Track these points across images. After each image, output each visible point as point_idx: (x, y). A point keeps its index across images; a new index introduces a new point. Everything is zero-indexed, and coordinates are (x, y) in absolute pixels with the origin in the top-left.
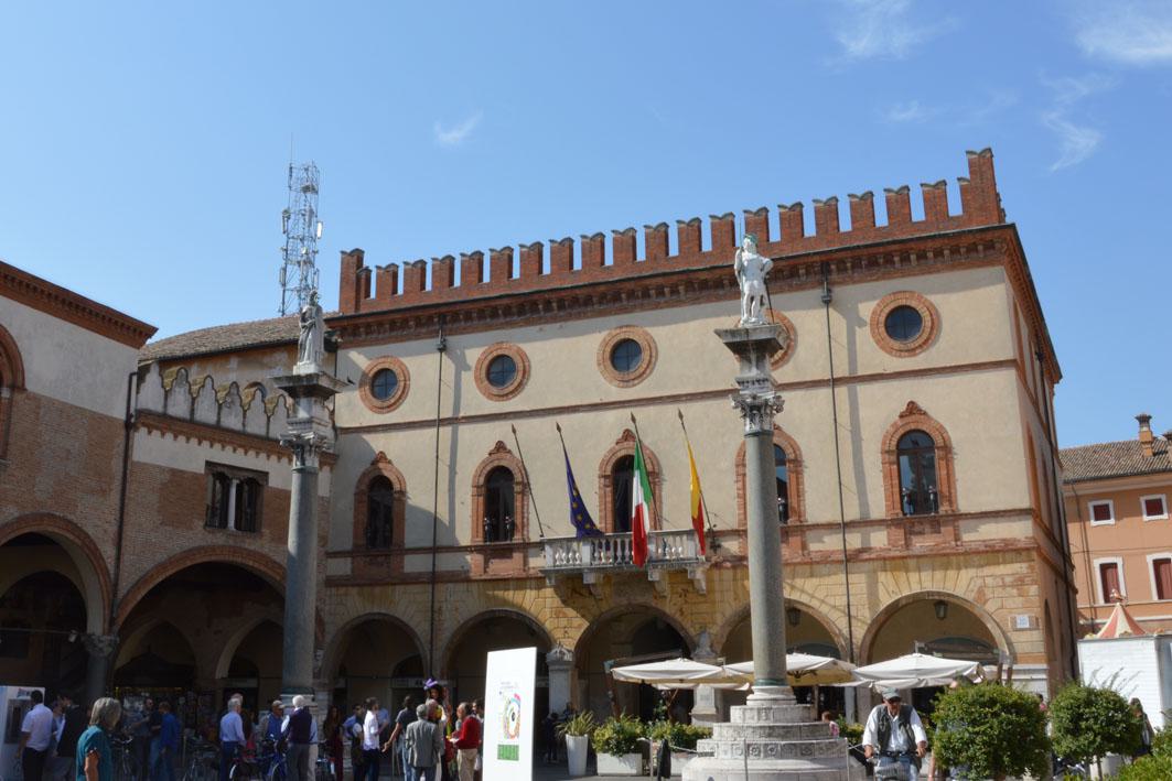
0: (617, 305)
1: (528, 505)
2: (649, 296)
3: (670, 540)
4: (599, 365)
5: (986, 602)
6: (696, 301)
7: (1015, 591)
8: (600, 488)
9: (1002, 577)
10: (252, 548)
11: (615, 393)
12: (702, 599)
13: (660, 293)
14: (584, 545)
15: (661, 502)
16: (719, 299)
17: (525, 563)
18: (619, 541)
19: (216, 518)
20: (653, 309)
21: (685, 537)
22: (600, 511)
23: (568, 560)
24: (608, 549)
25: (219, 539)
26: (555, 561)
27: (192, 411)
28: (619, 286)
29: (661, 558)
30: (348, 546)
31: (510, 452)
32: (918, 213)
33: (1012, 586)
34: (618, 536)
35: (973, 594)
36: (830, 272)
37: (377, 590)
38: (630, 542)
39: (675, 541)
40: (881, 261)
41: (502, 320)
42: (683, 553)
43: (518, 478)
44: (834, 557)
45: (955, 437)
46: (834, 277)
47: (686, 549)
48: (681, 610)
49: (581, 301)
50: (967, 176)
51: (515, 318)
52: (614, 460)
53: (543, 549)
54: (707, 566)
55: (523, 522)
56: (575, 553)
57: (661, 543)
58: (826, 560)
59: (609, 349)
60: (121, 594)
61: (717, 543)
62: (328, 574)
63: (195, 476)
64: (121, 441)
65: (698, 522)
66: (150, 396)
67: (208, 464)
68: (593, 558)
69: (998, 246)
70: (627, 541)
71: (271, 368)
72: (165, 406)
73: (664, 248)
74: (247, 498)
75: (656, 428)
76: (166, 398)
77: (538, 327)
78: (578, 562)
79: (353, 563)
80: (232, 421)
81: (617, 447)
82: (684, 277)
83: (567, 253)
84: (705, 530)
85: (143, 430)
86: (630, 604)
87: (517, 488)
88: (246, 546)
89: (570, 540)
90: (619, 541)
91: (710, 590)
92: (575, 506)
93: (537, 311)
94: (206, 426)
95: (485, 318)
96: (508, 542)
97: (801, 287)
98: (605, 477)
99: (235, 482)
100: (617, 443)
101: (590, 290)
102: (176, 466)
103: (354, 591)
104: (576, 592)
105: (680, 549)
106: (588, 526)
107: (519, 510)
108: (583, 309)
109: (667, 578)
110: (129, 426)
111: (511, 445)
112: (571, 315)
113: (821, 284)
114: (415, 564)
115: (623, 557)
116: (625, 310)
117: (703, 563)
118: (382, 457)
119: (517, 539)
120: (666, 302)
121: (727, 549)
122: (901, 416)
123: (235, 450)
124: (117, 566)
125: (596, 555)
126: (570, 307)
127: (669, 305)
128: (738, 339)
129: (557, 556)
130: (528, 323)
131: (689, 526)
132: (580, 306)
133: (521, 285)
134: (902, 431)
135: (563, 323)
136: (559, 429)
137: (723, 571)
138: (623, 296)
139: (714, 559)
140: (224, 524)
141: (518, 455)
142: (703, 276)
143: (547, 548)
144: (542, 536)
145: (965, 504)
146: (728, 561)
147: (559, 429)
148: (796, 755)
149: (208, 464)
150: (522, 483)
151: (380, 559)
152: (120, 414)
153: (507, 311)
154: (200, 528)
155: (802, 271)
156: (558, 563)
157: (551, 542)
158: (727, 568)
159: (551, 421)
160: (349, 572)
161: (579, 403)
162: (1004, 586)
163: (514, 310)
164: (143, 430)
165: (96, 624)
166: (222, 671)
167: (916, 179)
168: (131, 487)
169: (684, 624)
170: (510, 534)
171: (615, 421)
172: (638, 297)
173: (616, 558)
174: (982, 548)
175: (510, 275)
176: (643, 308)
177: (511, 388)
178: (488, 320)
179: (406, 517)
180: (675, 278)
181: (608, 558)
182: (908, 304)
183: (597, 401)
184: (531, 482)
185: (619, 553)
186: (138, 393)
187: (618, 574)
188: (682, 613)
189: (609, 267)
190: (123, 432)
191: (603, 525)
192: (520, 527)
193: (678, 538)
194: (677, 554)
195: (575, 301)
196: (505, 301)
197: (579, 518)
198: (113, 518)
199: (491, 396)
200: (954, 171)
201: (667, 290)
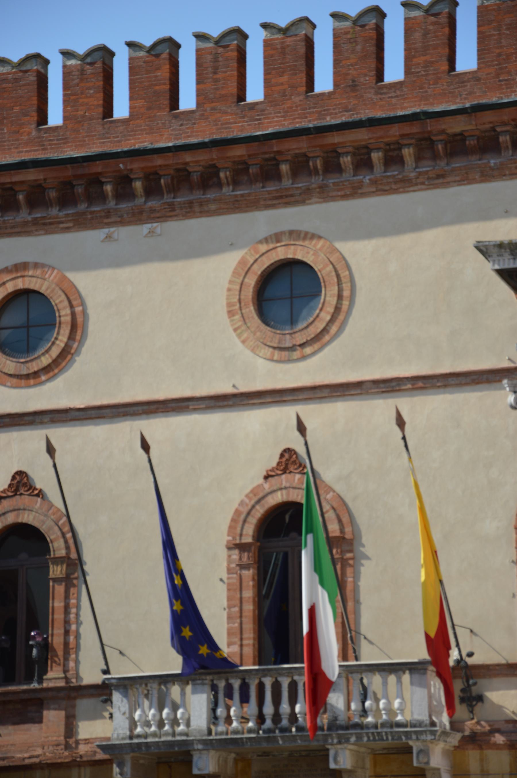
0: (272, 187)
1: (78, 607)
2: (339, 169)
3: (375, 682)
4: (231, 313)
6: (439, 180)
8: (229, 571)
13: (363, 163)
14: (194, 692)
15: (357, 602)
16: (487, 176)
17: (70, 730)
18: (268, 682)
20: (345, 197)
21: (406, 677)
22: (230, 618)
23: (161, 724)
24: (245, 699)
26: (133, 724)
28: (276, 146)
29: (356, 720)
31: (40, 494)
34: (265, 673)
38: (293, 686)
39: (385, 683)
41: (24, 215)
42: (402, 710)
43: (58, 548)
47: (411, 702)
49: (195, 177)
51: (54, 211)
52: (260, 511)
53: (108, 700)
54: (455, 739)
55: (66, 644)
56: (175, 708)
57: (356, 690)
59: (252, 281)
61: (475, 691)
65: (439, 642)
68: (214, 718)
70: (285, 682)
73: (446, 51)
75: (352, 452)
77: (101, 234)
78: (182, 728)
81: (267, 486)
82: (415, 129)
83: (164, 73)
84: (451, 662)
87: (56, 571)
90: (268, 682)
92: (178, 607)
93: (103, 197)
96: (35, 685)
98: (242, 547)
101: (215, 154)
105: (396, 703)
106: (204, 650)
107: (59, 616)
108: (197, 195)
109: (368, 764)
111: (42, 478)
112: (172, 207)
115: (277, 717)
116: (284, 199)
117: (444, 733)
119: (54, 678)
120: (374, 182)
121: (500, 707)
125: (220, 711)
126: (174, 189)
127: (382, 188)
129: (137, 715)
130: (81, 223)
131: (420, 653)
132: (191, 189)
133: (65, 141)
136: (145, 446)
137: (490, 753)
138: (284, 168)
139: (469, 725)
141: (59, 504)
142: (457, 126)
143: (116, 697)
144: (106, 672)
146: (498, 731)
147: (145, 446)
150: (66, 560)
153: (37, 197)
156: (139, 730)
157: (127, 684)
158: (496, 746)
159: (128, 430)
161: (187, 393)
163: (53, 194)
170: (39, 666)
171: (264, 431)
172: (316, 172)
173: (261, 719)
175: (42, 117)
176: (325, 194)
177: (45, 361)
180: (395, 131)
181: (244, 719)
183: (226, 389)
184: (87, 557)
185: (268, 709)
187: (265, 754)
189: (254, 105)
191: (236, 648)
192: (60, 653)
193: (392, 679)
194: (390, 711)
195: (182, 179)
196: (31, 175)
197: (187, 633)
201: (376, 156)
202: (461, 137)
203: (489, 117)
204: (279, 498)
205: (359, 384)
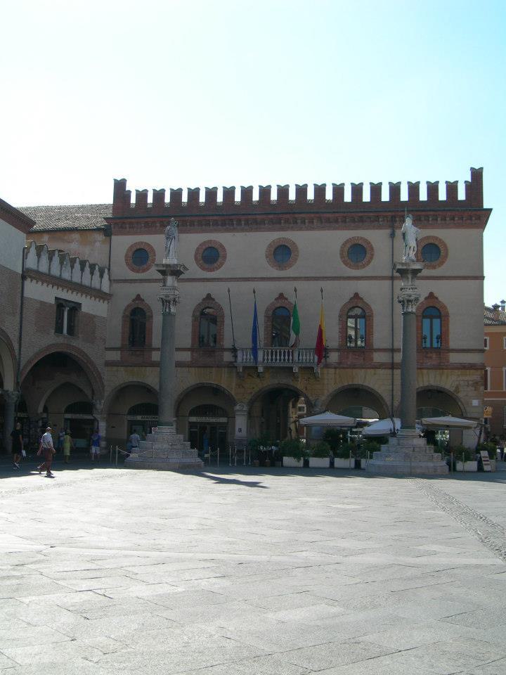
6: (323, 228)
7: (474, 388)
11: (276, 273)
13: (303, 222)
16: (335, 229)
19: (59, 329)
25: (60, 340)
26: (243, 360)
30: (118, 344)
36: (396, 221)
37: (136, 369)
45: (451, 310)
48: (306, 388)
51: (220, 227)
58: (381, 366)
59: (273, 249)
60: (21, 368)
63: (51, 305)
64: (20, 285)
66: (31, 262)
67: (57, 299)
71: (69, 242)
72: (38, 266)
74: (66, 315)
77: (232, 234)
79: (121, 354)
80: (66, 275)
82: (317, 215)
85: (29, 279)
88: (72, 344)
94: (54, 277)
95: (202, 225)
97: (380, 227)
100: (276, 299)
101: (264, 216)
102: (42, 300)
103: (122, 369)
104: (251, 376)
110: (24, 278)
118: (138, 297)
122: (426, 298)
123: (67, 291)
124: (20, 354)
130: (227, 230)
135: (247, 233)
140: (61, 332)
148: (240, 462)
149: (57, 299)
151: (138, 353)
152: (20, 271)
153: (216, 223)
162: (468, 386)
163: (220, 223)
164: (29, 279)
165: (9, 385)
166: (40, 409)
167: (442, 178)
168: (25, 311)
176: (292, 229)
178: (204, 227)
186: (26, 258)
196: (215, 218)
198: (17, 328)
199: (203, 269)
201: (306, 221)
202: (329, 218)
203: (337, 215)
204: (279, 305)
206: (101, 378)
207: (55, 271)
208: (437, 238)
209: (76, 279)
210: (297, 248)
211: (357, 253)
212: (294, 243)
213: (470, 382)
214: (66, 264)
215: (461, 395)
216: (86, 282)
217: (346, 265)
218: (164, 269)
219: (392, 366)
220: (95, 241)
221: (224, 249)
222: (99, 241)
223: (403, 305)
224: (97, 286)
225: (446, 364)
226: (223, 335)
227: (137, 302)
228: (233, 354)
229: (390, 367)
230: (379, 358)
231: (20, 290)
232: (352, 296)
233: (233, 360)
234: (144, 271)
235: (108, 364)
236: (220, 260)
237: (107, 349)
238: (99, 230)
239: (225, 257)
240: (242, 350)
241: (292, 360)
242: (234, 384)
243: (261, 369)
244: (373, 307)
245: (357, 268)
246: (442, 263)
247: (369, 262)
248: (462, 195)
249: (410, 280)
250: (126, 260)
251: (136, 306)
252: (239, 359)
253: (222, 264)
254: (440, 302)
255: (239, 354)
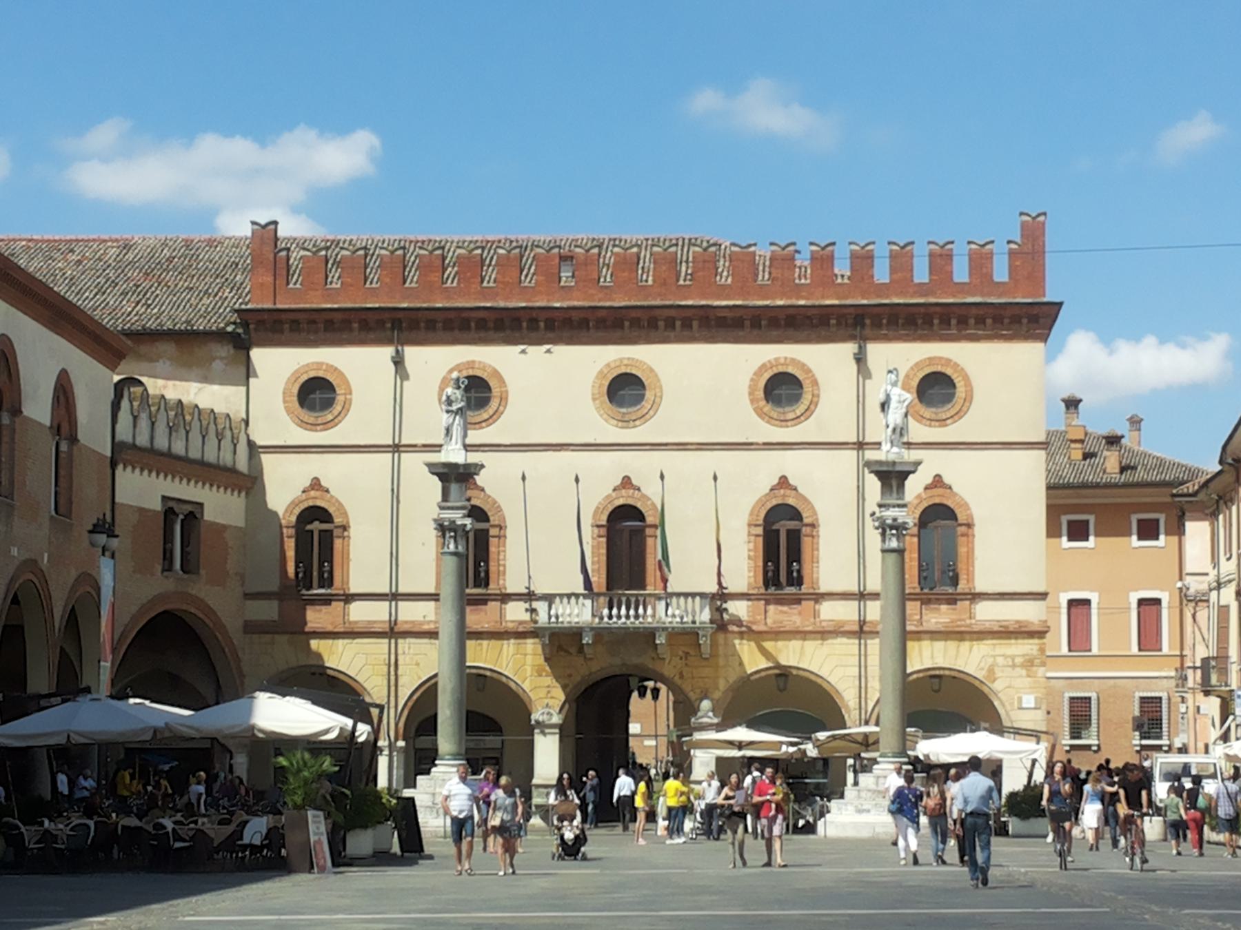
4: (594, 399)
5: (994, 681)
7: (1024, 672)
8: (593, 538)
9: (1013, 657)
10: (194, 592)
12: (704, 663)
26: (550, 617)
27: (152, 438)
32: (961, 272)
33: (1022, 666)
35: (984, 672)
36: (863, 326)
40: (920, 321)
44: (847, 628)
46: (867, 331)
50: (1018, 240)
51: (491, 333)
52: (610, 508)
62: (247, 618)
67: (164, 498)
69: (1042, 321)
76: (135, 426)
79: (280, 607)
80: (179, 448)
81: (614, 495)
86: (624, 664)
89: (577, 596)
91: (714, 655)
99: (181, 517)
103: (284, 638)
113: (851, 338)
114: (360, 612)
122: (926, 488)
128: (885, 469)
134: (925, 504)
138: (627, 324)
145: (981, 584)
149: (164, 498)
152: (109, 454)
154: (159, 573)
155: (833, 322)
160: (276, 618)
162: (1014, 666)
164: (120, 467)
169: (684, 686)
174: (996, 628)
177: (485, 416)
179: (351, 556)
182: (943, 370)
188: (682, 676)
190: (109, 471)
200: (1003, 233)
205: (666, 444)
206: (238, 660)
207: (161, 443)
208: (948, 361)
209: (194, 454)
210: (659, 380)
211: (782, 389)
212: (652, 370)
213: (1018, 660)
214: (179, 425)
215: (998, 686)
216: (211, 456)
217: (760, 413)
218: (445, 470)
219: (862, 631)
220: (213, 359)
221: (502, 381)
222: (222, 358)
223: (883, 534)
224: (229, 463)
225: (968, 622)
226: (504, 566)
227: (313, 493)
228: (527, 606)
229: (856, 628)
230: (831, 612)
231: (109, 493)
232: (775, 481)
233: (527, 617)
234: (327, 425)
235: (251, 628)
236: (494, 404)
237: (248, 596)
238: (219, 336)
239: (504, 399)
240: (549, 598)
241: (653, 616)
242: (529, 669)
243: (587, 640)
244: (818, 506)
245: (784, 422)
246: (959, 415)
247: (808, 412)
248: (1001, 272)
249: (895, 489)
250: (285, 402)
251: (311, 503)
252: (542, 618)
253: (497, 414)
254: (956, 494)
255: (541, 606)
